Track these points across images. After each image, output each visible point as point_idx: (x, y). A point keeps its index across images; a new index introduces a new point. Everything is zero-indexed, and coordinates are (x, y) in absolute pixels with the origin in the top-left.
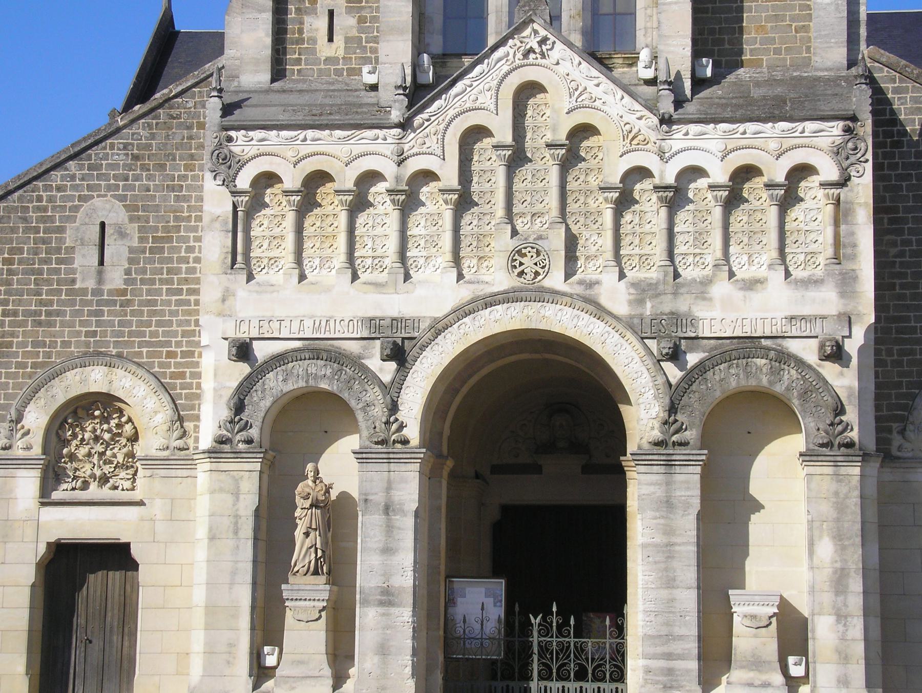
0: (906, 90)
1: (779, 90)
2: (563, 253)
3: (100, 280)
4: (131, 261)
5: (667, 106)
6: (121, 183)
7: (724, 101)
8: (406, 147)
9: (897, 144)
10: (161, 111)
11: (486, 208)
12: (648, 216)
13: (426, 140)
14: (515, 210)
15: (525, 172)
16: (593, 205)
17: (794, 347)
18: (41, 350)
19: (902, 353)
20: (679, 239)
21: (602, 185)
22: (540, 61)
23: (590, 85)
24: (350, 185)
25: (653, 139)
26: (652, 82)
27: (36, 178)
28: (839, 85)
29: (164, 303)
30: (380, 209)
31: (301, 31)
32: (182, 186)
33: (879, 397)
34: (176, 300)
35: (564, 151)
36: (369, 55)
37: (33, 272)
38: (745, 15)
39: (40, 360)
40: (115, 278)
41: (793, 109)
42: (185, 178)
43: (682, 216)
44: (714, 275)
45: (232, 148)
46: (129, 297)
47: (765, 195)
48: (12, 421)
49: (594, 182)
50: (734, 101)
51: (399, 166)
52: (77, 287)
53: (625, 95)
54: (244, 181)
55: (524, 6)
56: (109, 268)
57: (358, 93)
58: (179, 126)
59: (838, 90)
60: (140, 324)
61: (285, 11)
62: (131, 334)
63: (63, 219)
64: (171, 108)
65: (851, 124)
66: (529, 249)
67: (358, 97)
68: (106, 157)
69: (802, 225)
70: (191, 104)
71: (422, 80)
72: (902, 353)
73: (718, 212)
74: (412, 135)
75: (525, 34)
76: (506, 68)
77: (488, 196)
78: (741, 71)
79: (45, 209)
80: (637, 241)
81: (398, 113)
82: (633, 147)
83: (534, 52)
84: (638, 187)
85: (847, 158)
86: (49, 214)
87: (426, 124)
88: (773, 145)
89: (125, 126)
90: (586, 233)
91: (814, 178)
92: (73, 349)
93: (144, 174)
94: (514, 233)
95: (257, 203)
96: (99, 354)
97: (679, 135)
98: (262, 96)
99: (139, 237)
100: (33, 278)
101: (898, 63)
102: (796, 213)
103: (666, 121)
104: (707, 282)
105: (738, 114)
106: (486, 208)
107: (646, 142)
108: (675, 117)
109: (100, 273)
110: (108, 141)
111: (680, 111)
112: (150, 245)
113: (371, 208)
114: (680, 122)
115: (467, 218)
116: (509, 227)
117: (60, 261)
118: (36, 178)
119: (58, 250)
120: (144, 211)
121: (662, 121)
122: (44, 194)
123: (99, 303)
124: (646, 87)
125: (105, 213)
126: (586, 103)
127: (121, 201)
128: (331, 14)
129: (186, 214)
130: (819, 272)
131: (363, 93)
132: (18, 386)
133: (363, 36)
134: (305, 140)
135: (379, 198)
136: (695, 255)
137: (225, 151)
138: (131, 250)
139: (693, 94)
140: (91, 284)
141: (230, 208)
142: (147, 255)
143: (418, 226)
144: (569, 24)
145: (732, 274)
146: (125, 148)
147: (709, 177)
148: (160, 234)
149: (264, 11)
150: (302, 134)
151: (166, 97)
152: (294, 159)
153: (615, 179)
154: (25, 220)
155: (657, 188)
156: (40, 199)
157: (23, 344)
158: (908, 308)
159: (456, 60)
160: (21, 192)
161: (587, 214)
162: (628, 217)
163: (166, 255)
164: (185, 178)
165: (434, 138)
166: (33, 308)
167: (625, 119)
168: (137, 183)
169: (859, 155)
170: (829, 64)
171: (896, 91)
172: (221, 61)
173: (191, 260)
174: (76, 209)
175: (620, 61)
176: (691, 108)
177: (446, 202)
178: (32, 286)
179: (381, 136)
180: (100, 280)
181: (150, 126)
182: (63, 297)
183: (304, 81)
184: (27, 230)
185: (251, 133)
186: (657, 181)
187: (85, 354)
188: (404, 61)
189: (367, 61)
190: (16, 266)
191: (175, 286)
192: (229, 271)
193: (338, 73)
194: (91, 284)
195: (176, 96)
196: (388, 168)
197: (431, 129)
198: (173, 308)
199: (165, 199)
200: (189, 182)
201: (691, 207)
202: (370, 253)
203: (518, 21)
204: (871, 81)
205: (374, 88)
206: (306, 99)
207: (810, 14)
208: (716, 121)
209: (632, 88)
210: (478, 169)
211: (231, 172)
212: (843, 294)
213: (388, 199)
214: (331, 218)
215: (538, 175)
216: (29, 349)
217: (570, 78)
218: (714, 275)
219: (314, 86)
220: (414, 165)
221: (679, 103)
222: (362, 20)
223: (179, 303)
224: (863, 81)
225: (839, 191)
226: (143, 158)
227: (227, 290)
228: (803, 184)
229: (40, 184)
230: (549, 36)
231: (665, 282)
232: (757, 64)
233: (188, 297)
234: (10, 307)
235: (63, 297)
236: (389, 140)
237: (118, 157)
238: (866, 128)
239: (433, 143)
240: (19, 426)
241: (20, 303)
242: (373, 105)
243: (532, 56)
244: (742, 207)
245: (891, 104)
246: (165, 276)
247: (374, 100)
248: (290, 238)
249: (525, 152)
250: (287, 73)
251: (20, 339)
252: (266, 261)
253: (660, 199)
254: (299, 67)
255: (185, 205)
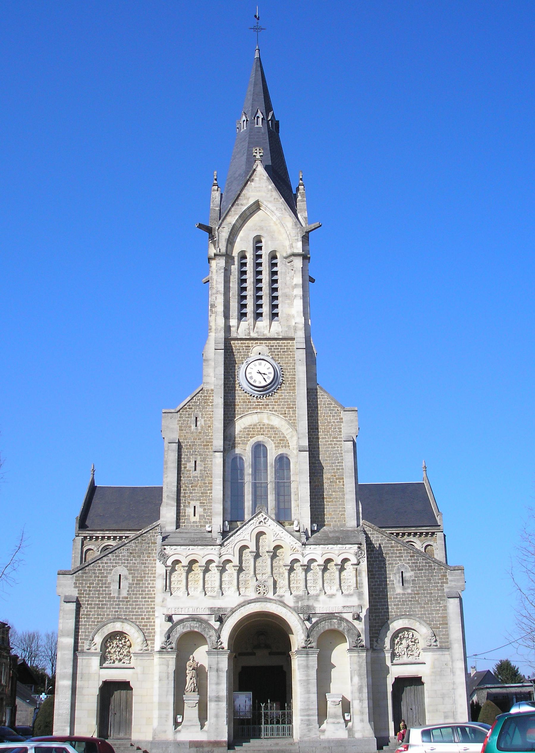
0: (374, 534)
1: (337, 534)
2: (273, 586)
3: (119, 594)
4: (129, 587)
5: (304, 540)
6: (126, 562)
7: (321, 538)
8: (222, 552)
9: (372, 551)
10: (139, 538)
11: (246, 572)
12: (299, 575)
13: (228, 550)
14: (257, 572)
15: (259, 560)
16: (281, 570)
17: (345, 616)
18: (100, 617)
19: (376, 616)
20: (308, 582)
21: (285, 565)
22: (264, 525)
23: (280, 533)
24: (204, 564)
25: (300, 550)
26: (299, 531)
27: (98, 560)
28: (355, 533)
29: (140, 601)
30: (213, 572)
31: (185, 513)
32: (146, 563)
33: (370, 630)
34: (144, 601)
35: (272, 554)
36: (207, 521)
37: (97, 591)
38: (325, 510)
39: (100, 620)
40: (124, 593)
41: (342, 541)
42: (147, 560)
43: (309, 574)
44: (320, 593)
45: (165, 552)
46: (129, 599)
47: (335, 567)
48: (90, 640)
49: (281, 563)
50: (324, 538)
51: (220, 558)
52: (111, 596)
53: (291, 536)
54: (169, 563)
55: (258, 507)
56: (122, 590)
57: (204, 533)
58: (145, 543)
59: (355, 535)
60: (132, 608)
61: (180, 506)
62: (129, 612)
63: (107, 573)
64: (143, 537)
65: (360, 546)
66: (262, 585)
67: (205, 535)
68: (121, 553)
69: (346, 577)
70: (149, 536)
71: (225, 530)
72: (376, 616)
73: (320, 573)
74: (224, 548)
75: (259, 516)
76: (254, 527)
77: (248, 567)
78: (325, 527)
79: (101, 570)
80: (295, 582)
81: (219, 541)
82: (294, 552)
83: (262, 522)
84: (295, 565)
85: (359, 556)
86: (103, 571)
87: (228, 544)
88: (337, 552)
89: (128, 543)
90: (279, 580)
91: (349, 562)
92: (110, 616)
93: (134, 559)
94: (257, 580)
95: (173, 570)
96: (119, 618)
97: (308, 549)
98: (174, 534)
99: (132, 580)
100: (97, 593)
101: (372, 525)
102: (344, 573)
103: (304, 544)
104: (318, 595)
105: (326, 543)
106: (247, 572)
107: (298, 551)
108: (307, 543)
109: (119, 591)
110: (122, 548)
111: (308, 541)
112: (136, 582)
113: (210, 572)
114: (308, 545)
115: (241, 575)
116: (255, 578)
117: (106, 587)
118: (98, 560)
119: (105, 584)
120: (133, 571)
121: (303, 544)
122: (101, 565)
123: (119, 601)
124: (296, 532)
125: (121, 571)
126: (279, 538)
127: (126, 567)
128: (195, 507)
129: (147, 572)
130: (352, 592)
131: (206, 534)
132: (92, 629)
133: (205, 514)
134: (189, 549)
135: (213, 568)
136: (314, 587)
137: (163, 553)
138: (129, 584)
139: (311, 536)
140: (116, 595)
141: (165, 571)
142: (135, 585)
143: (226, 577)
144: (271, 512)
145: (325, 593)
146: (127, 550)
147: (317, 562)
148: (139, 579)
149: (174, 506)
150: (188, 547)
151: (141, 534)
152: (186, 556)
153: (288, 563)
154: (95, 573)
155: (301, 566)
156: (99, 566)
157: (94, 615)
158: (377, 602)
159: (235, 523)
160: (93, 564)
161: (280, 574)
162: (292, 575)
163: (141, 585)
164: (147, 560)
165: (231, 549)
166: (97, 603)
167: (292, 543)
168: (131, 562)
169: (362, 555)
170: (351, 526)
171: (371, 534)
172: (159, 522)
173: (149, 587)
174: (111, 570)
175: (287, 524)
176: (311, 540)
177: (235, 570)
178: (97, 595)
179: (214, 549)
180: (119, 594)
181: (136, 543)
182: (107, 599)
183: (187, 529)
184: (95, 577)
185: (172, 547)
186: (301, 563)
187: (115, 618)
188: (220, 524)
189: (207, 523)
190: (91, 589)
191: (144, 596)
192: (165, 592)
193: (197, 526)
194: (116, 595)
195: (144, 533)
196: (216, 558)
197: (230, 546)
198: (143, 603)
199: (141, 567)
200: (148, 561)
201: (312, 571)
202: (210, 586)
203: (257, 512)
204: (365, 532)
205: (210, 532)
206: (188, 535)
207: (345, 510)
208: (319, 545)
209: (292, 533)
210: (244, 559)
211: (165, 560)
212: (359, 599)
213: (216, 569)
214: (197, 575)
215: (264, 561)
216: (96, 616)
217: (274, 530)
218: (320, 593)
219: (190, 531)
220: (224, 558)
221: (307, 539)
222: (205, 509)
223: (145, 601)
224: (363, 532)
225: (357, 566)
226: (134, 554)
227: (164, 598)
228: (346, 564)
229: (100, 561)
230: (267, 517)
231: (305, 596)
232: (330, 525)
233: (148, 600)
234: (90, 602)
235: (107, 599)
236: (216, 550)
237: (125, 553)
238: (364, 547)
239: (230, 551)
240: (93, 642)
241: (93, 601)
242: (210, 538)
243: (261, 523)
244: (328, 571)
245: (370, 538)
246: (140, 592)
247: (210, 536)
248: (184, 581)
249: (259, 554)
250: (181, 526)
251: (93, 613)
252: (176, 589)
253: (303, 569)
254: (184, 524)
255: (147, 569)
